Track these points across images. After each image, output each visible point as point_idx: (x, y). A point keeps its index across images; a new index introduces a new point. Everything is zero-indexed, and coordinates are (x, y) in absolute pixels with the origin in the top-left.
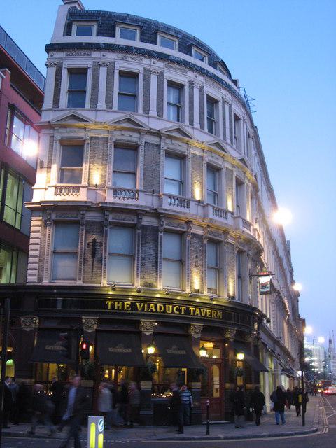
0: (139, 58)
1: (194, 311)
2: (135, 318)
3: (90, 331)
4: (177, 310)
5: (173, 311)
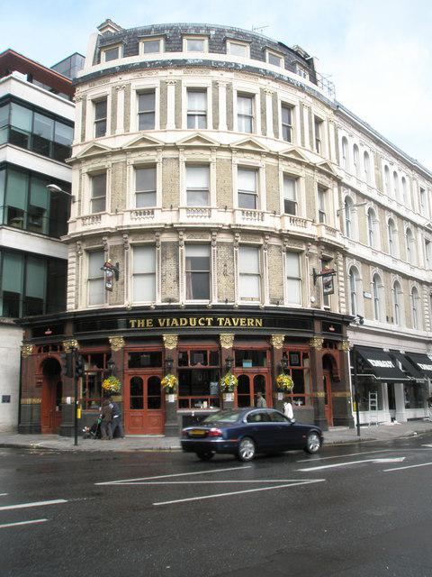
0: (154, 73)
1: (224, 322)
2: (158, 334)
3: (117, 350)
4: (202, 322)
5: (197, 324)
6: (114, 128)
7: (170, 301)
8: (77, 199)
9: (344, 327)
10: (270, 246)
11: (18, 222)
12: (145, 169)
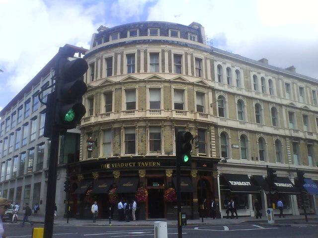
5: (128, 166)
6: (97, 77)
7: (116, 155)
9: (214, 165)
10: (165, 126)
12: (108, 96)
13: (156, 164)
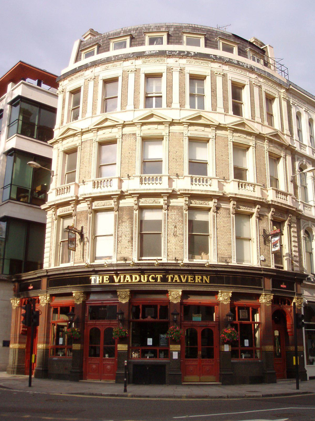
0: (118, 63)
1: (172, 279)
2: (113, 289)
4: (153, 278)
5: (148, 281)
6: (85, 112)
8: (55, 174)
11: (24, 197)
13: (202, 280)
